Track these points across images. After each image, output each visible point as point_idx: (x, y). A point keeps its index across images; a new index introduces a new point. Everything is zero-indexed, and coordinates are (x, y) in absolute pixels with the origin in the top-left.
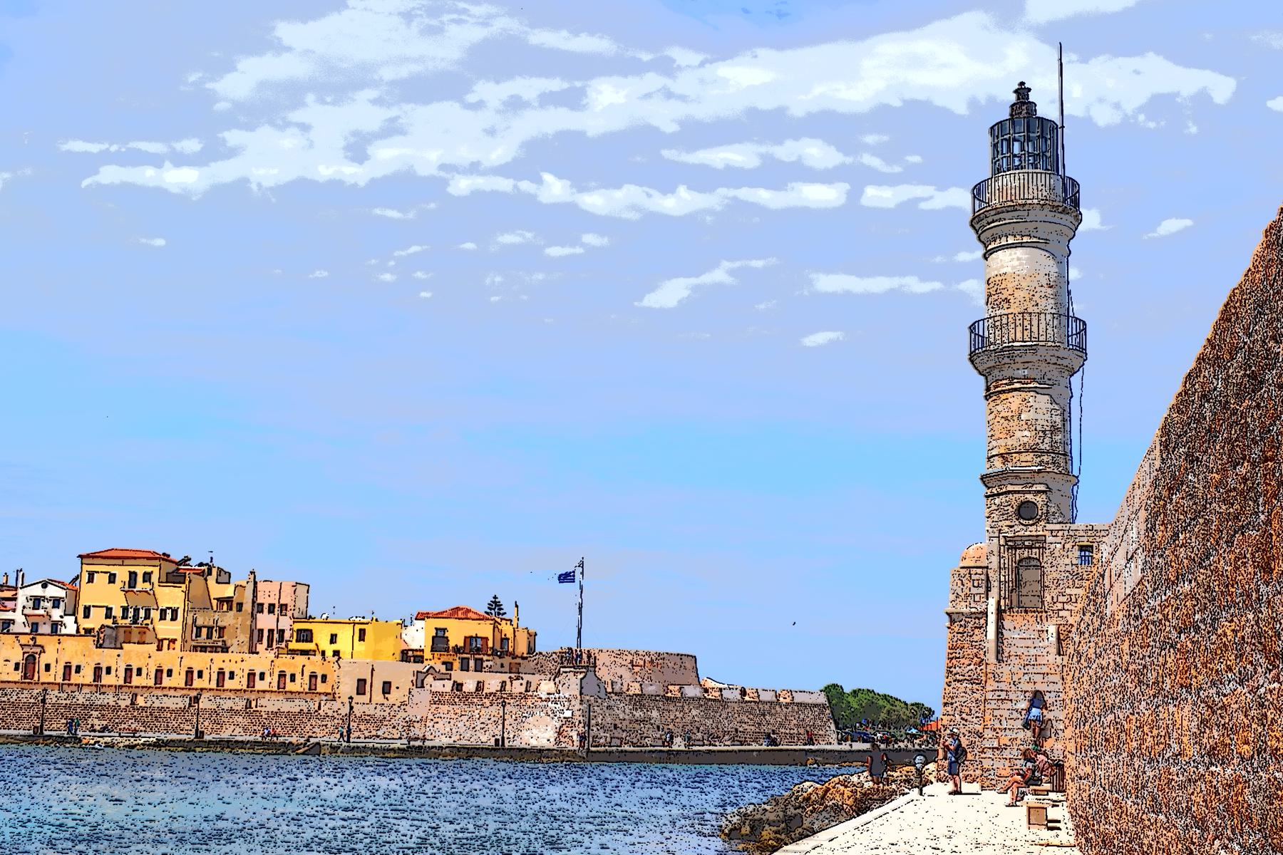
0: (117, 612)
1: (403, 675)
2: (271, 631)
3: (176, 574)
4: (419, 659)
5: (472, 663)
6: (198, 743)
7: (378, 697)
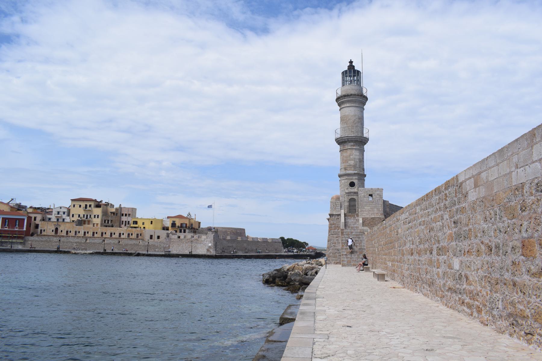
1: (163, 233)
2: (126, 222)
3: (98, 205)
4: (168, 229)
5: (183, 231)
7: (156, 239)
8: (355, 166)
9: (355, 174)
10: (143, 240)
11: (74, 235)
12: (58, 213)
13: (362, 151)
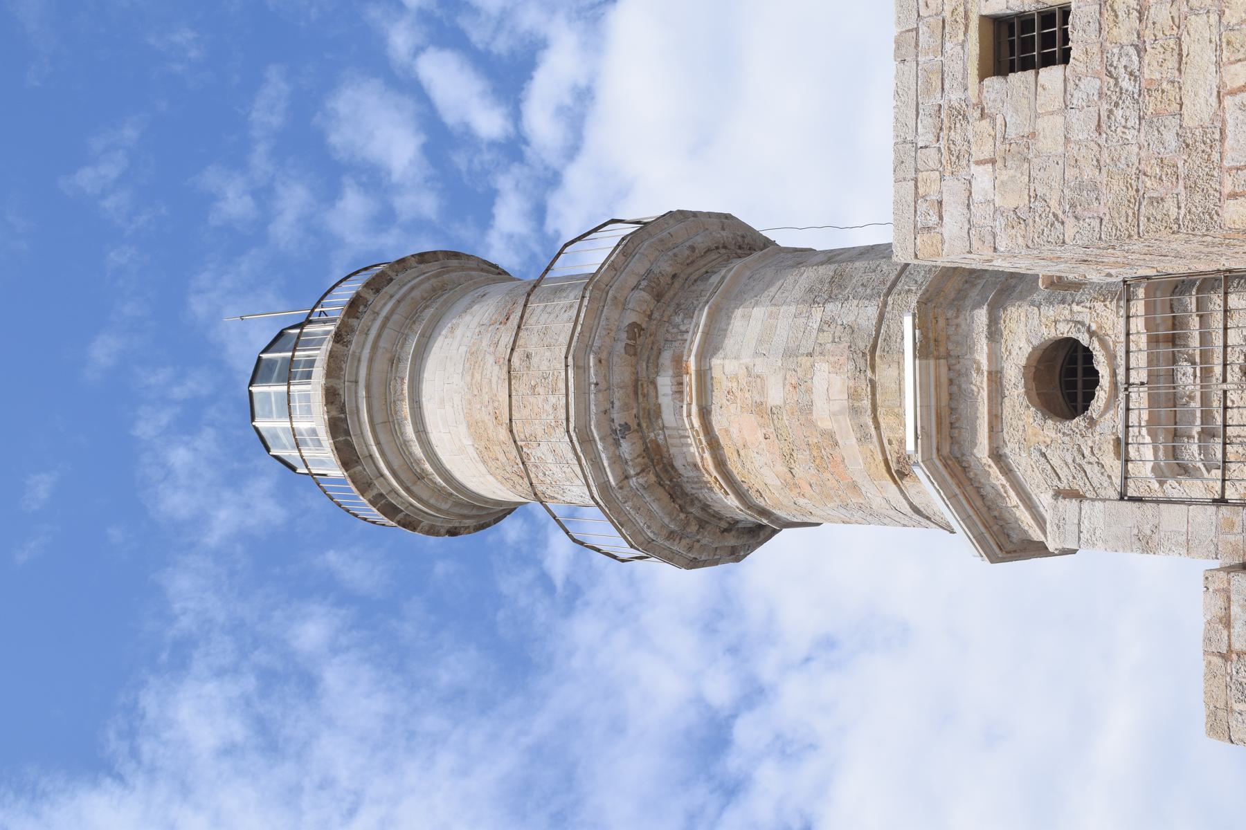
8: (872, 351)
9: (922, 351)
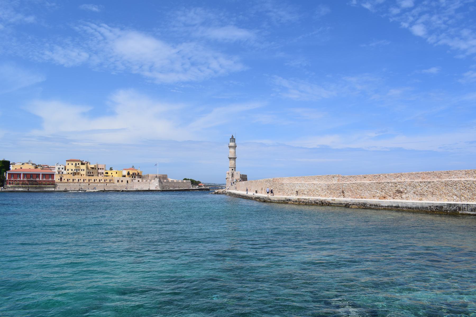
0: (73, 170)
6: (104, 191)
10: (114, 183)
11: (72, 181)
12: (59, 169)
13: (235, 161)
